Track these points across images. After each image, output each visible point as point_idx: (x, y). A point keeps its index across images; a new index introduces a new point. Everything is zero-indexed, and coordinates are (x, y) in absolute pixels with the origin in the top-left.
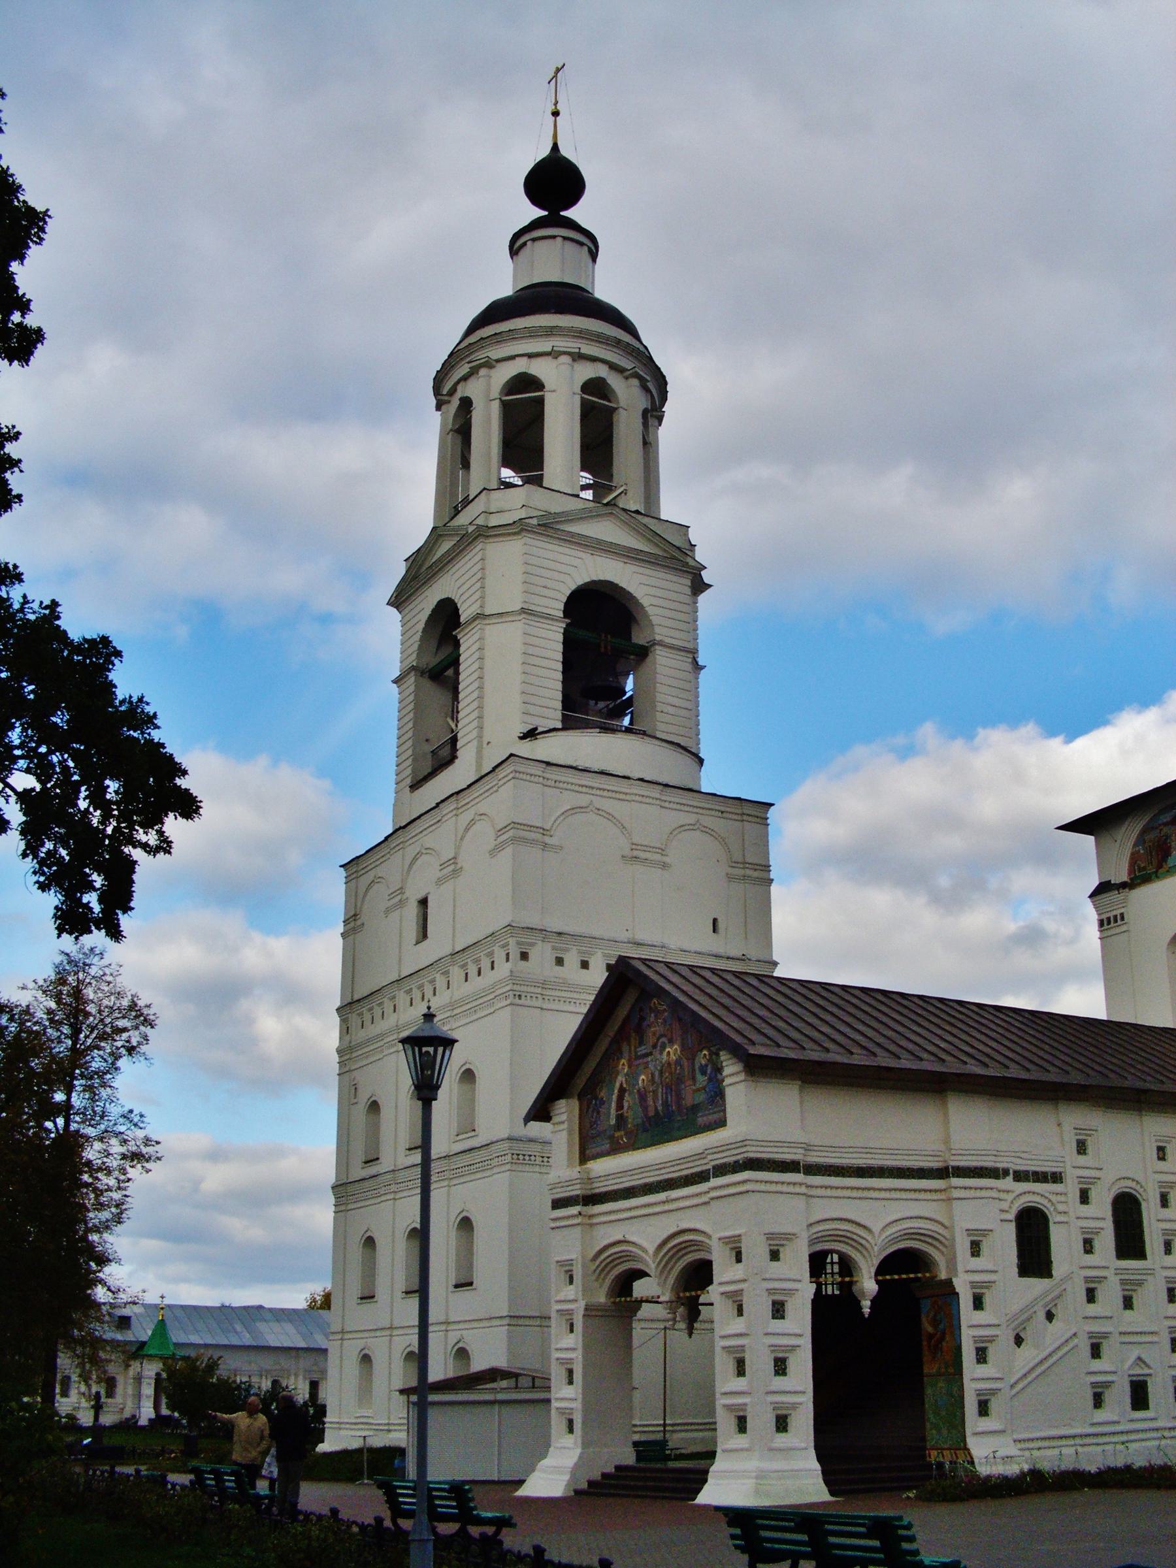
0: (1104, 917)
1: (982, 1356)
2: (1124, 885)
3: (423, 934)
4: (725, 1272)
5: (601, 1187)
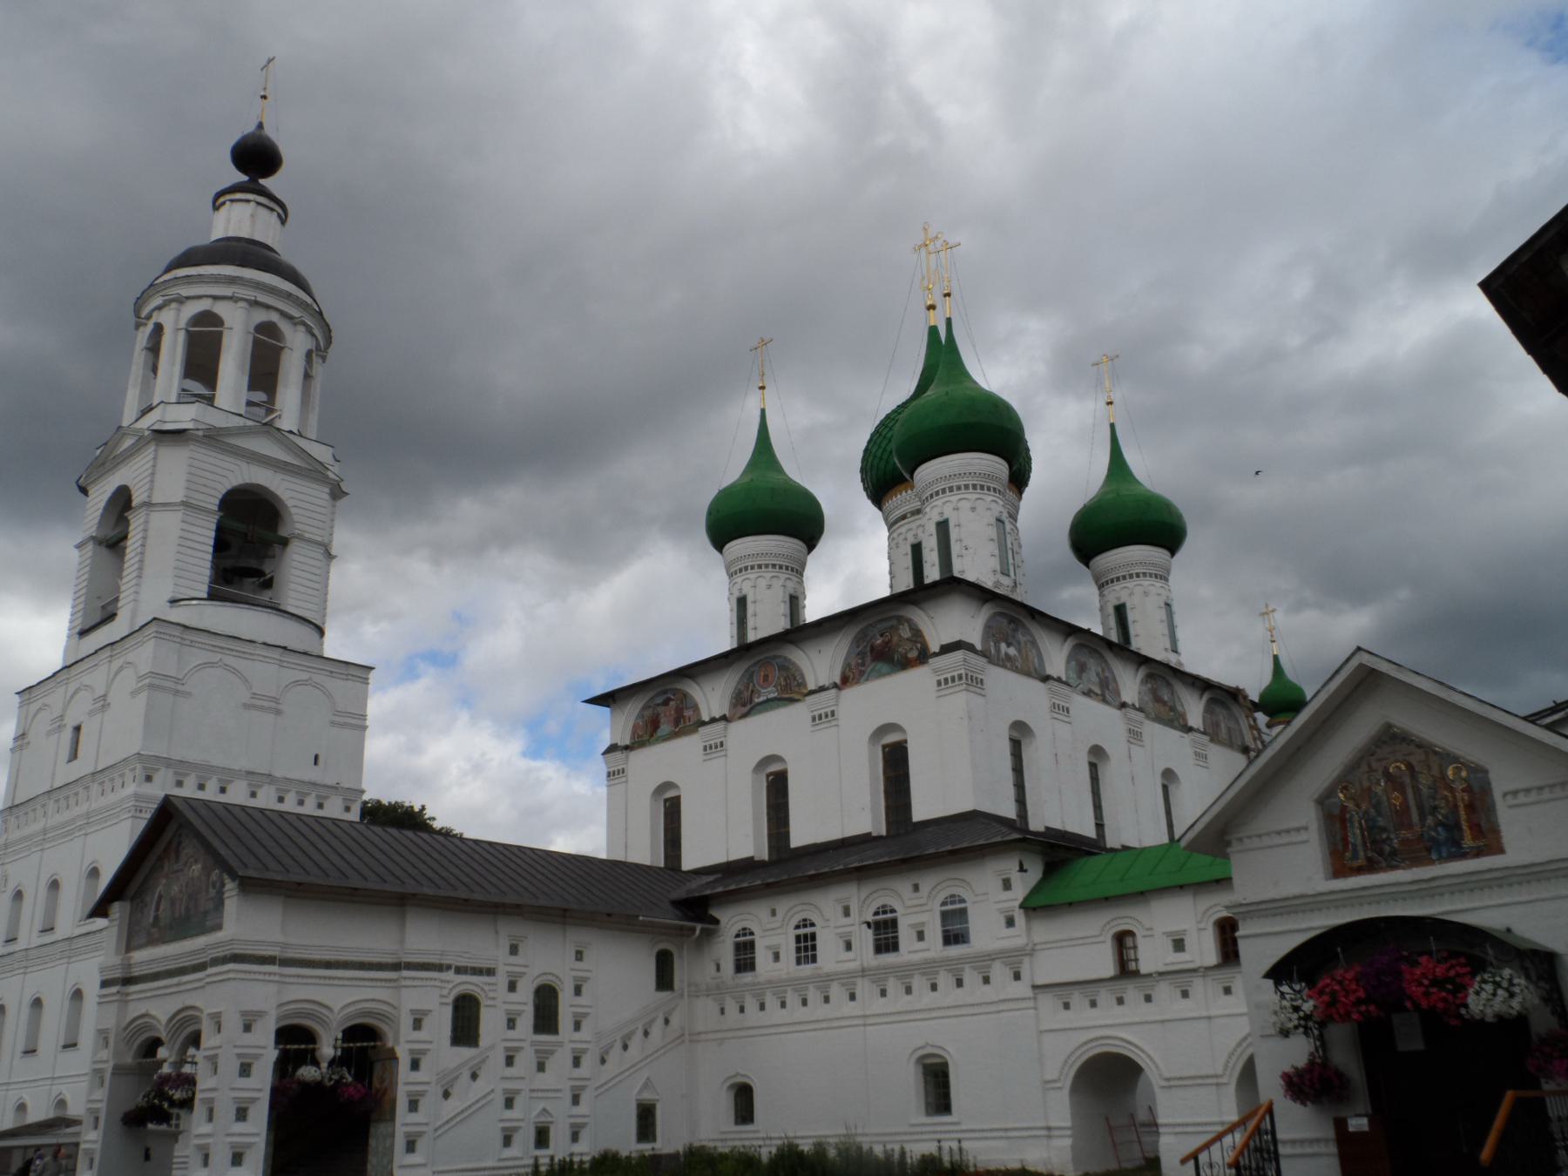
0: (611, 770)
1: (413, 1106)
2: (627, 748)
3: (74, 756)
4: (208, 1040)
5: (136, 972)
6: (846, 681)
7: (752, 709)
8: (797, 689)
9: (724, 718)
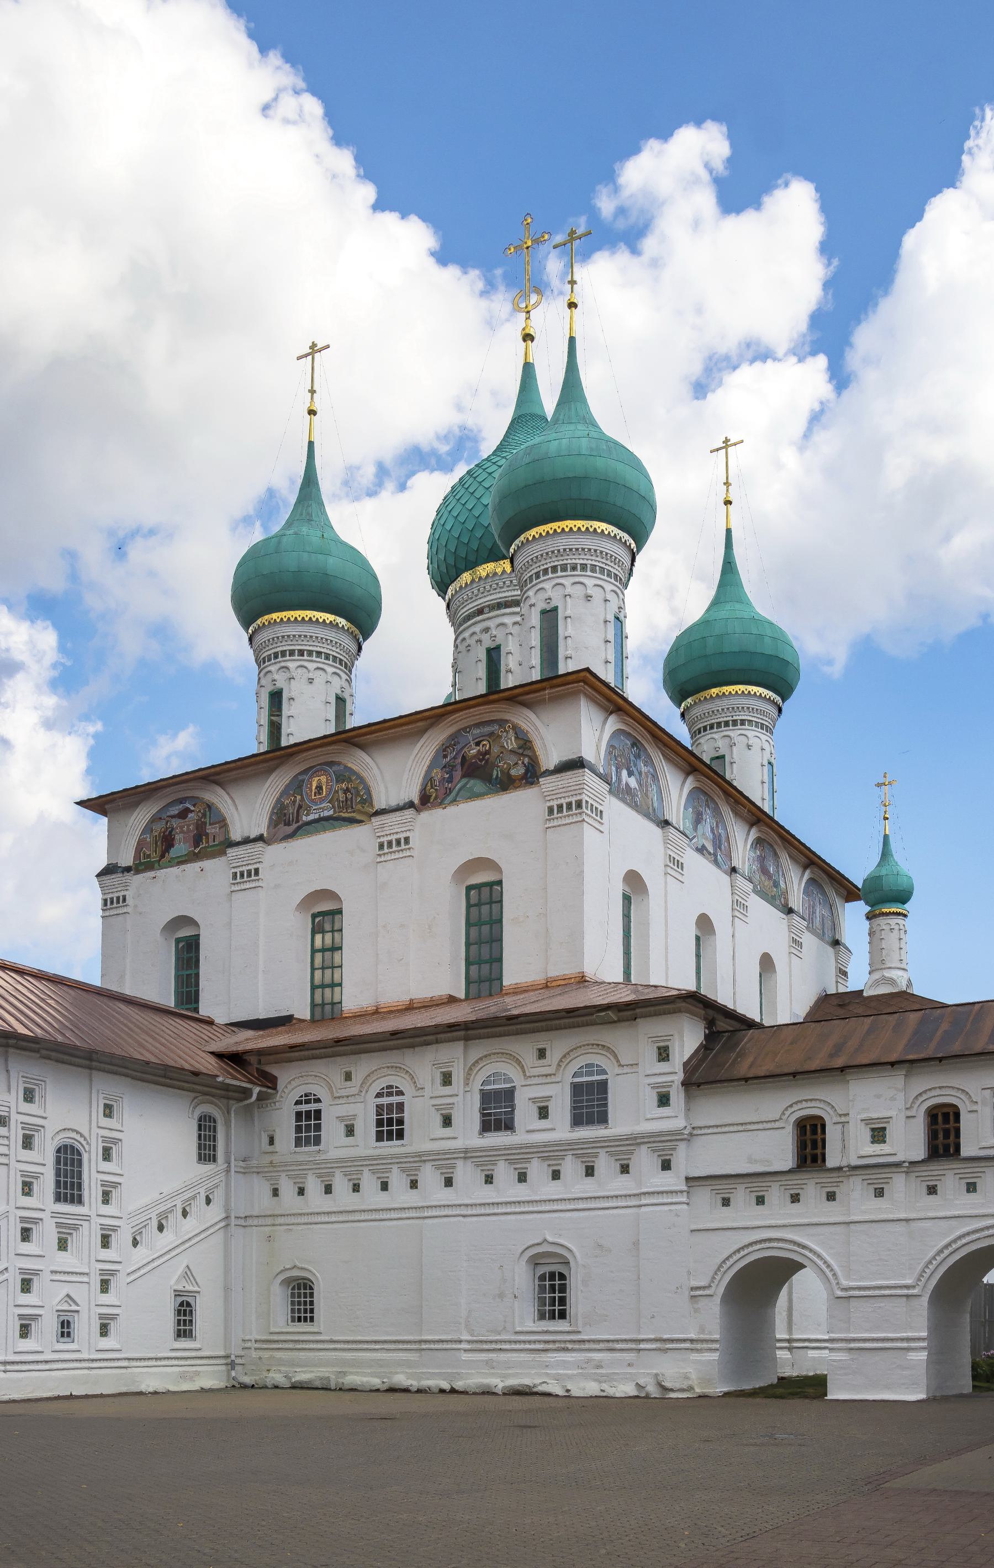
2: (128, 869)
6: (425, 801)
7: (299, 828)
8: (359, 807)
9: (260, 838)
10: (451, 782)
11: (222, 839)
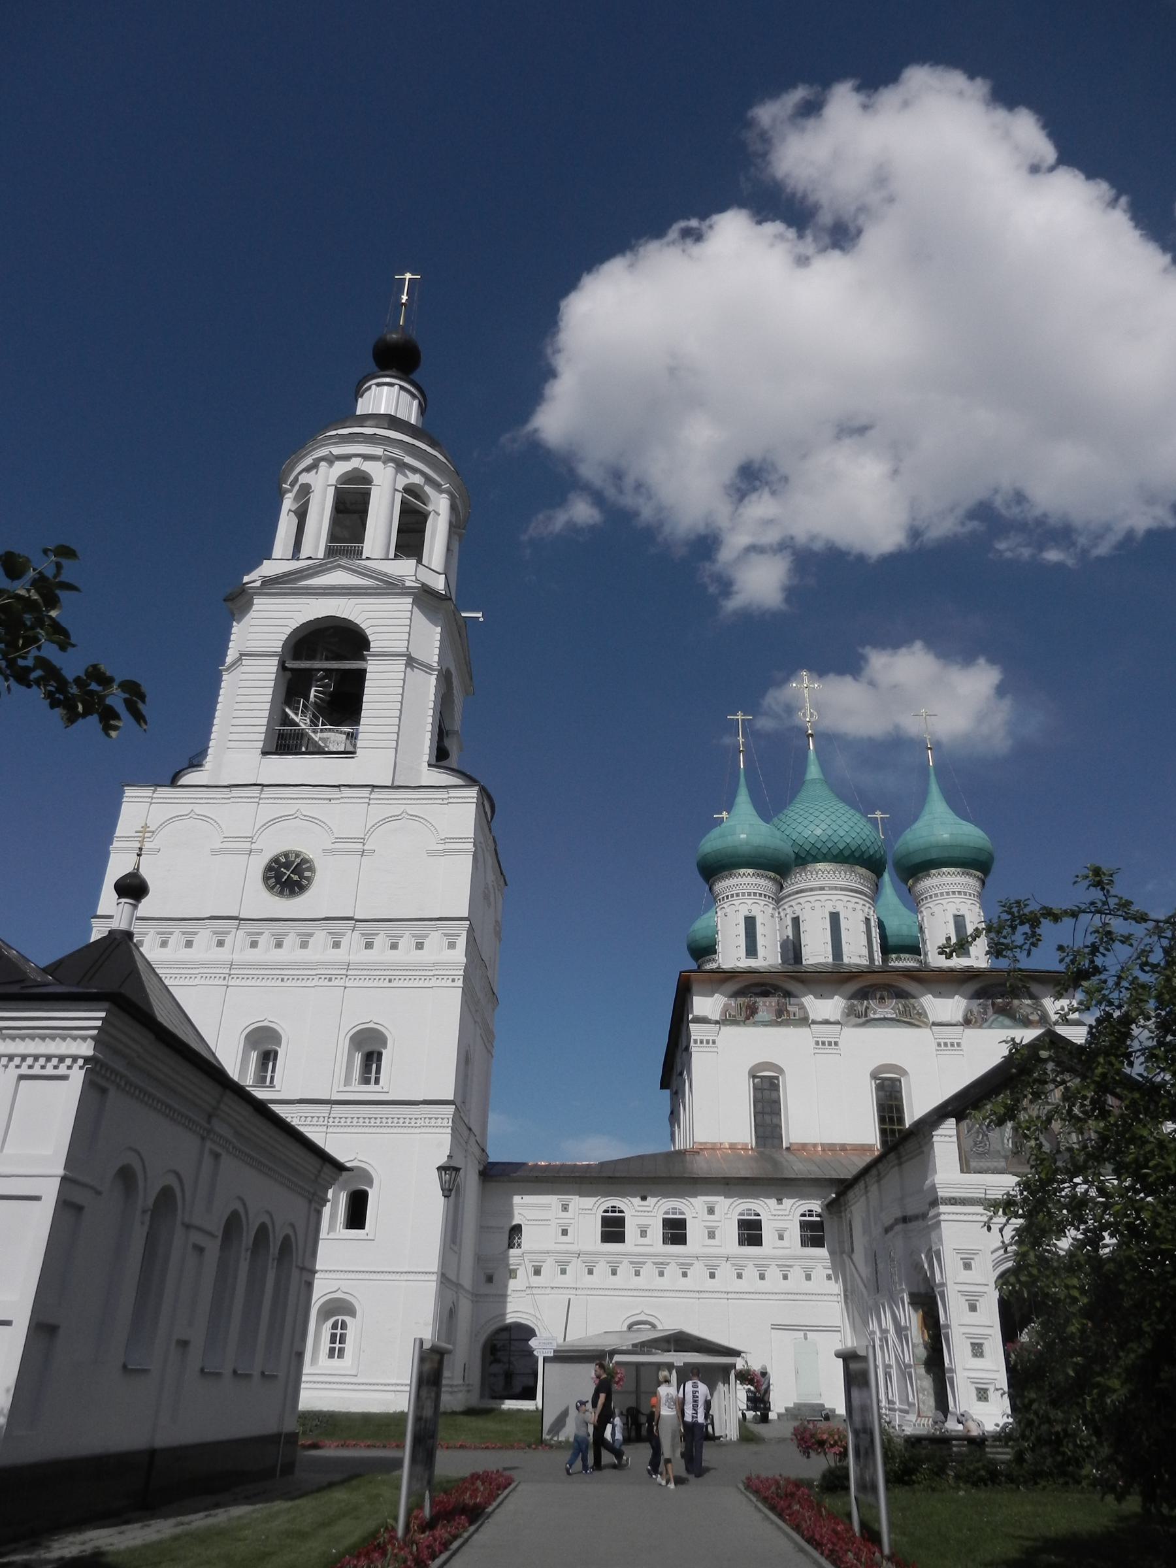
2: (717, 1022)
7: (868, 1021)
8: (917, 1017)
10: (986, 1014)
11: (802, 1016)
